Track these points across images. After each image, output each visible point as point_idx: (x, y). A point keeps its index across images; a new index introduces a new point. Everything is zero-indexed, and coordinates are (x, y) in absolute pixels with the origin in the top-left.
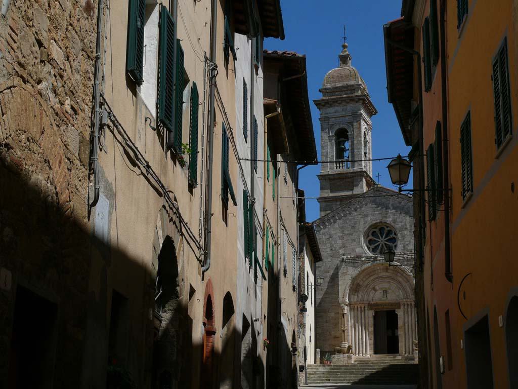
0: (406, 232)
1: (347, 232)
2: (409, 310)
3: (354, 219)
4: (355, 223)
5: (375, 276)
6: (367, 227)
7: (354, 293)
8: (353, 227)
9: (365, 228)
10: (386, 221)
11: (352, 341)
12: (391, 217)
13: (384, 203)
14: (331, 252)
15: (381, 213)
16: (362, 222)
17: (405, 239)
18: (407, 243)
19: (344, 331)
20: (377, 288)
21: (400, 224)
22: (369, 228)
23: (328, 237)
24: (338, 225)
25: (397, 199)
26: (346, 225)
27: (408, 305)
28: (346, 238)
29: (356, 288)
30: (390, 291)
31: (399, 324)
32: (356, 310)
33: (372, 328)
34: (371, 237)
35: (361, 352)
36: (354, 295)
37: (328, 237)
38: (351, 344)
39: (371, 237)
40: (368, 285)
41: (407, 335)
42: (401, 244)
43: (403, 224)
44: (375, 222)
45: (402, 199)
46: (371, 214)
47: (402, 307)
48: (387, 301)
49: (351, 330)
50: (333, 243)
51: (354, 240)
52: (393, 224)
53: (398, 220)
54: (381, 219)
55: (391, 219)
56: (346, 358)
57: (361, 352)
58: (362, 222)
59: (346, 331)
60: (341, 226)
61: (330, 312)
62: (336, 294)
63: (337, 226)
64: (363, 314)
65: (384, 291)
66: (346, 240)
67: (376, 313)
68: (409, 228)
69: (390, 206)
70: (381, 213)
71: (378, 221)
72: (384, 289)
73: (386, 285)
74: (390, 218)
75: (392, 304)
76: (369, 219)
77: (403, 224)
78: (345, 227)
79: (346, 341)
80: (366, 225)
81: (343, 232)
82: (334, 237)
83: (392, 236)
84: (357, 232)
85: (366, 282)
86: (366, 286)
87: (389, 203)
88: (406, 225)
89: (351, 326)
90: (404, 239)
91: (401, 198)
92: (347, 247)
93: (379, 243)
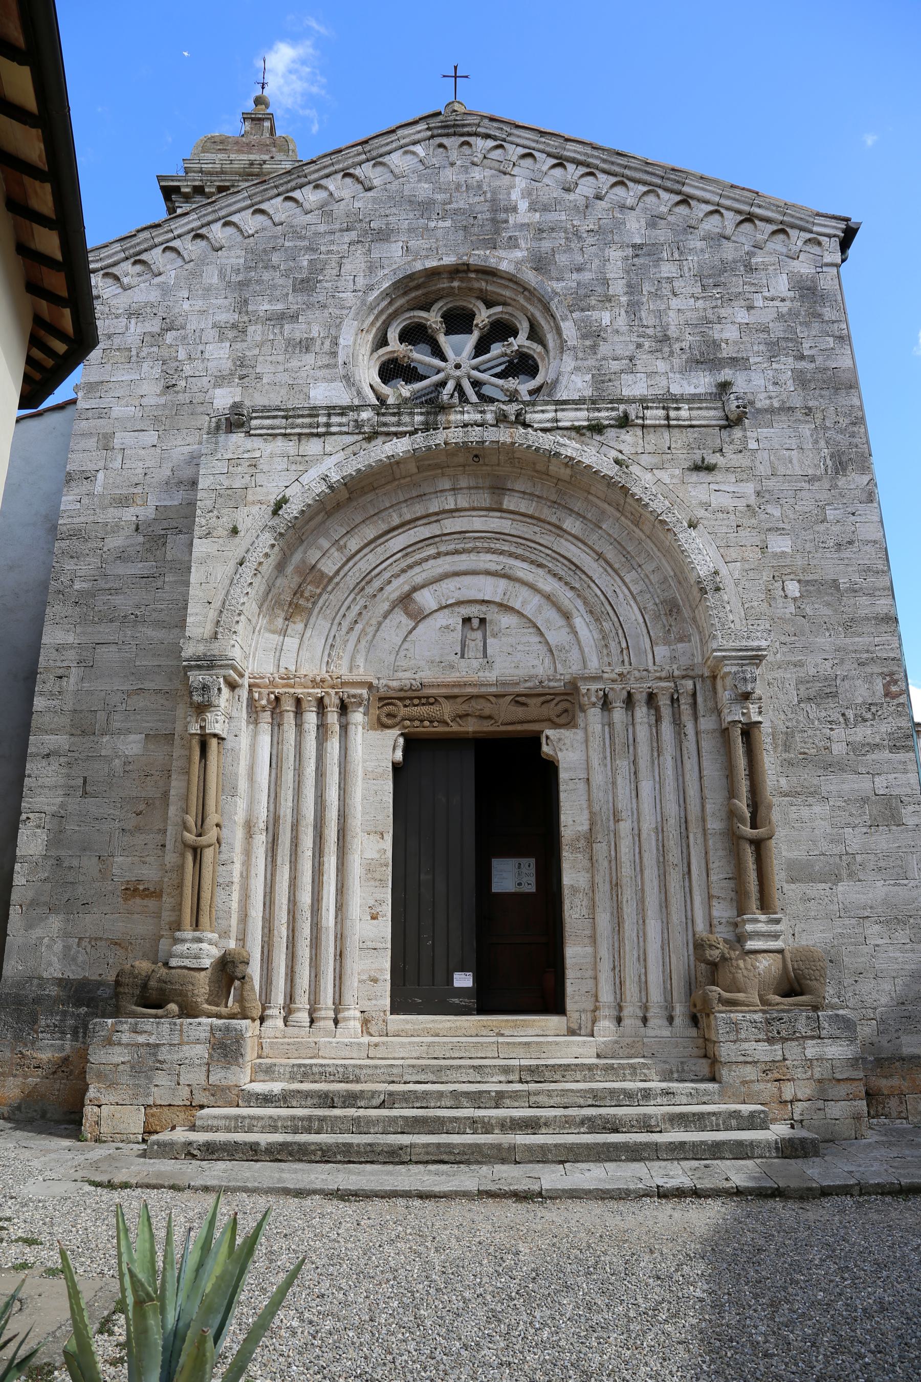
0: (606, 318)
1: (264, 306)
2: (643, 732)
3: (311, 249)
4: (316, 268)
5: (424, 532)
6: (386, 285)
7: (280, 622)
8: (306, 285)
9: (371, 288)
10: (492, 262)
11: (244, 918)
12: (523, 245)
13: (480, 187)
14: (162, 400)
15: (465, 228)
16: (356, 264)
17: (604, 349)
18: (615, 366)
19: (197, 852)
20: (426, 599)
21: (575, 276)
22: (386, 294)
23: (156, 329)
24: (222, 275)
25: (558, 172)
26: (266, 276)
27: (629, 701)
28: (256, 332)
29: (298, 592)
30: (507, 620)
31: (564, 818)
32: (289, 718)
33: (387, 844)
34: (395, 346)
35: (302, 1001)
36: (284, 633)
37: (154, 326)
38: (242, 939)
39: (395, 346)
40: (367, 578)
41: (628, 893)
42: (577, 369)
43: (587, 276)
44: (432, 263)
45: (583, 170)
46: (410, 230)
47: (594, 717)
48: (491, 676)
49: (248, 853)
50: (182, 355)
51: (305, 345)
52: (530, 277)
53: (562, 259)
54: (462, 250)
55: (519, 254)
56: (201, 1051)
57: (302, 1001)
58: (356, 264)
59: (208, 854)
60: (235, 278)
61: (120, 732)
62: (159, 624)
63: (215, 280)
64: (333, 746)
65: (467, 621)
66: (260, 345)
67: (412, 744)
68: (624, 299)
69: (515, 195)
70: (465, 228)
71: (449, 260)
72: (466, 611)
73: (491, 589)
74: (516, 246)
75: (519, 700)
76: (395, 250)
77: (587, 276)
78: (259, 282)
79: (204, 919)
80: (381, 273)
81: (242, 305)
82: (191, 327)
83: (521, 341)
84: (324, 306)
85: (364, 564)
86: (359, 588)
87: (513, 187)
88: (606, 282)
89: (249, 828)
90: (594, 348)
91: (579, 163)
92: (259, 378)
93: (442, 364)
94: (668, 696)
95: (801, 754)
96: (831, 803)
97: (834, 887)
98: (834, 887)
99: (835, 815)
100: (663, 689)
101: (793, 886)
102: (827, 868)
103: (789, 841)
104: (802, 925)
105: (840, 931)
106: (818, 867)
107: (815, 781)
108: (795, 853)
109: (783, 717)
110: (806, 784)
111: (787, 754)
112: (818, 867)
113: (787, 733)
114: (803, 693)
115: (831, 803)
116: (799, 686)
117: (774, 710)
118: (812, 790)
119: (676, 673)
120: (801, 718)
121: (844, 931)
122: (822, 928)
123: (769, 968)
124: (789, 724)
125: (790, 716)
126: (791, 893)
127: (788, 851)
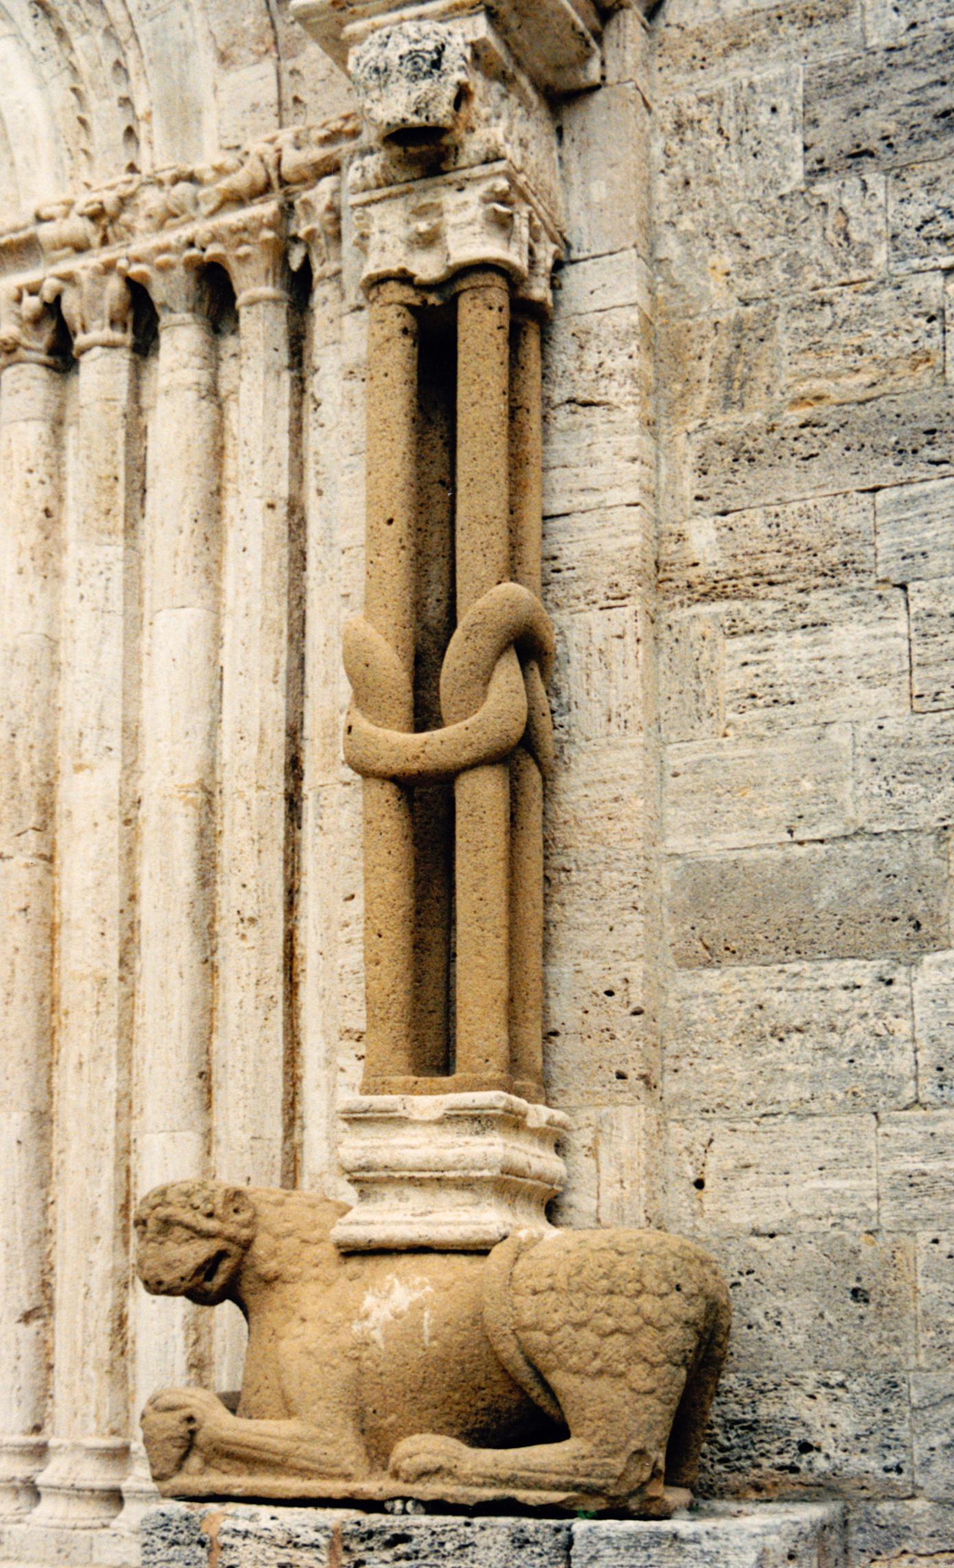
94: (262, 262)
95: (799, 401)
96: (919, 604)
97: (900, 975)
98: (900, 975)
99: (932, 652)
100: (241, 233)
101: (712, 979)
102: (874, 895)
103: (710, 787)
104: (739, 1143)
105: (911, 1163)
106: (828, 893)
107: (852, 516)
108: (733, 839)
109: (727, 259)
110: (807, 534)
111: (734, 414)
112: (828, 893)
113: (739, 326)
114: (830, 140)
115: (919, 604)
116: (817, 110)
117: (687, 239)
118: (834, 555)
119: (293, 160)
120: (813, 249)
121: (933, 1166)
122: (827, 1152)
123: (406, 1325)
124: (756, 285)
125: (761, 248)
126: (699, 1010)
127: (702, 829)
